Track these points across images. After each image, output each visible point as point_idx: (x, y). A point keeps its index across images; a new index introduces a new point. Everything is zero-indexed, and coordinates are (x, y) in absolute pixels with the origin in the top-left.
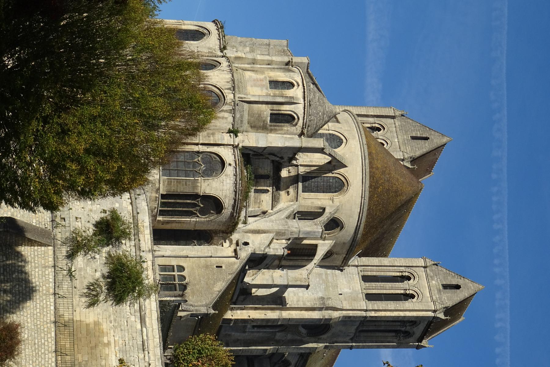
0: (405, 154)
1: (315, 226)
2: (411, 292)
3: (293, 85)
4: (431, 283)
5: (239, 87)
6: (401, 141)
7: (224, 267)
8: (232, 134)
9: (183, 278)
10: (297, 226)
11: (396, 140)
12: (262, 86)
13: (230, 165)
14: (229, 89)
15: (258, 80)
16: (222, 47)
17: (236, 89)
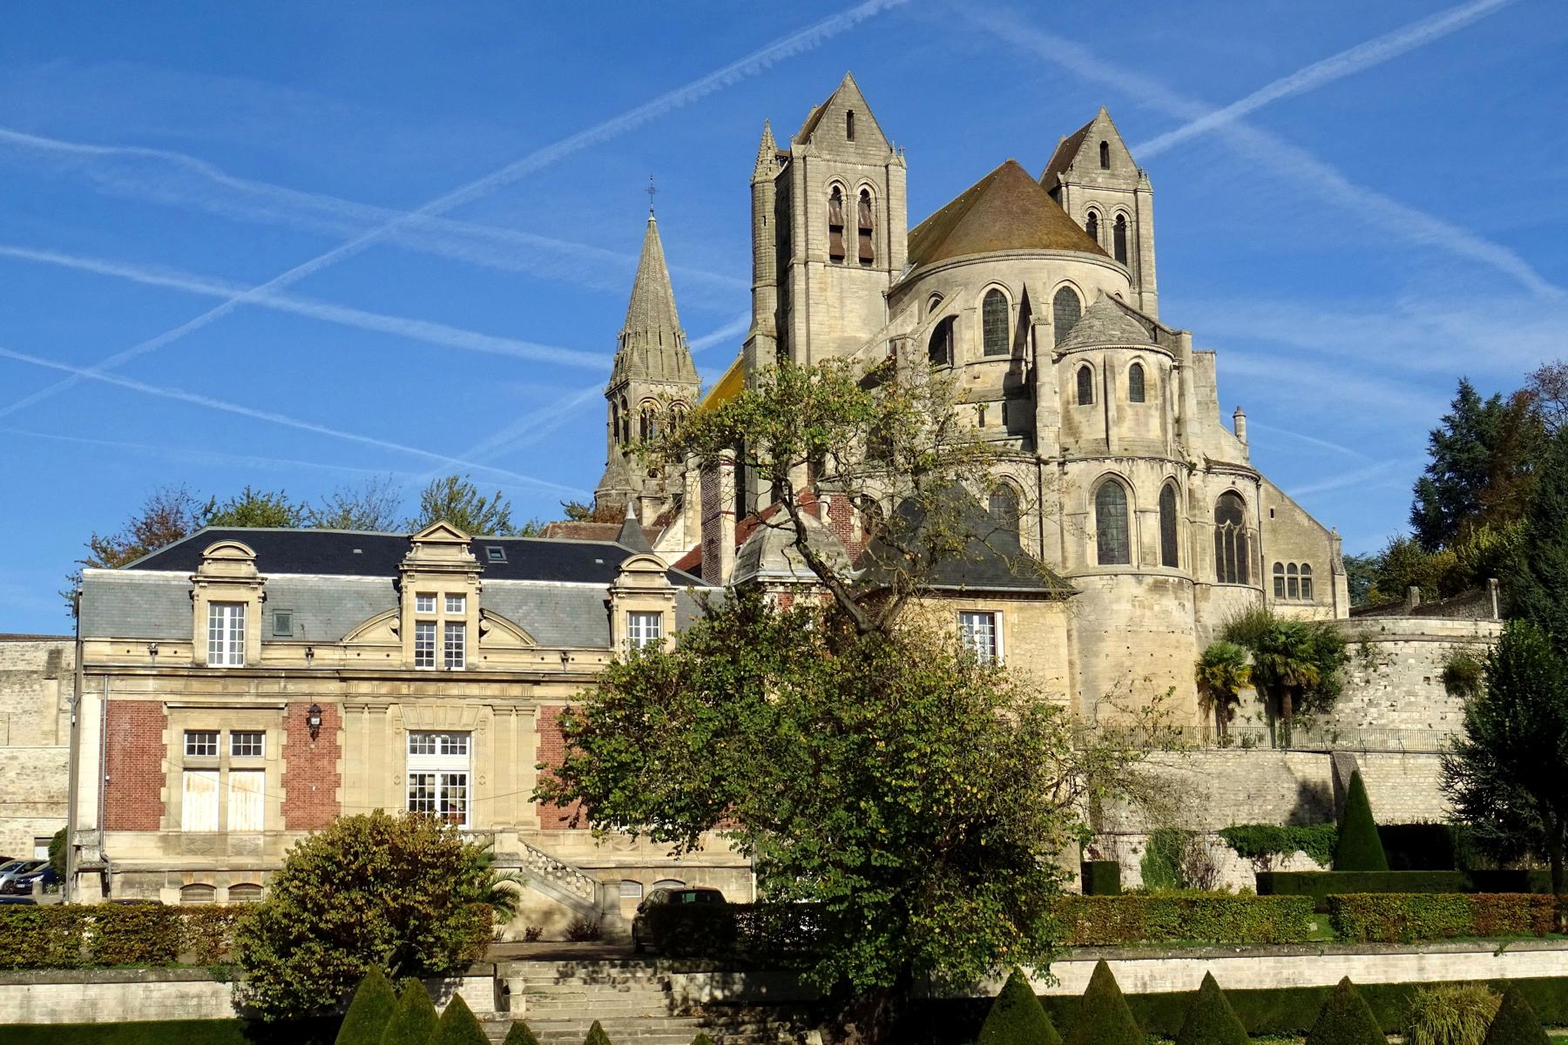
0: (892, 161)
1: (1206, 362)
2: (1114, 218)
3: (1138, 364)
4: (1101, 185)
5: (1158, 452)
6: (859, 159)
7: (1274, 507)
8: (1194, 472)
9: (1292, 567)
10: (1208, 389)
11: (860, 167)
12: (1147, 415)
13: (1233, 483)
14: (1161, 466)
15: (1138, 420)
16: (1034, 460)
17: (1164, 456)
